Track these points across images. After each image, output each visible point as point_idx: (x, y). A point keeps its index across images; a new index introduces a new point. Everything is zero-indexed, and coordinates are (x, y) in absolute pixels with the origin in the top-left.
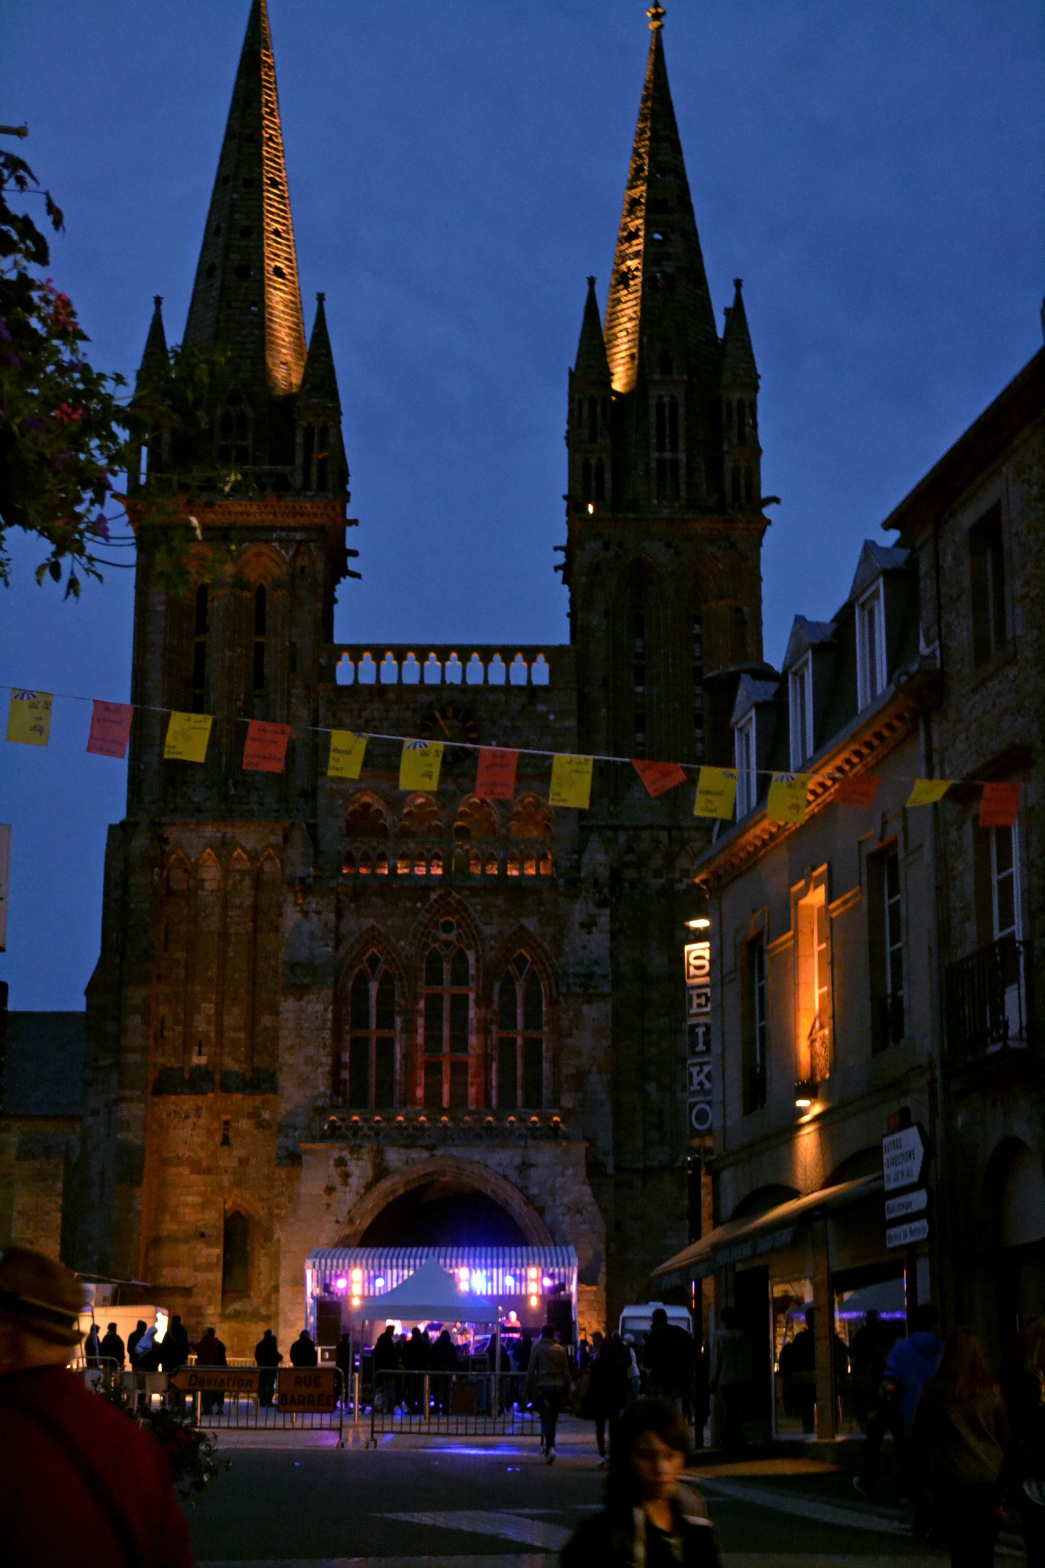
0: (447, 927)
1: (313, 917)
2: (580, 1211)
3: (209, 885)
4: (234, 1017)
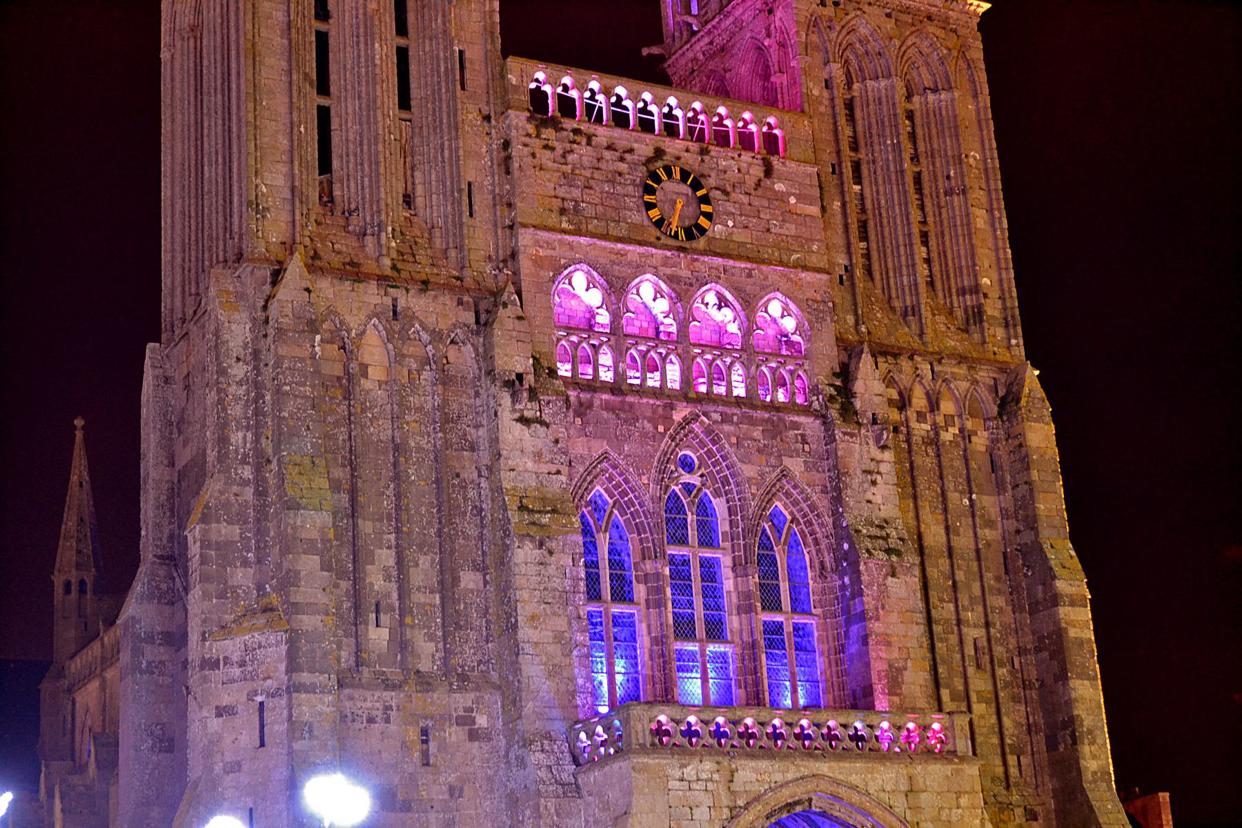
0: (687, 465)
3: (375, 373)
4: (424, 569)
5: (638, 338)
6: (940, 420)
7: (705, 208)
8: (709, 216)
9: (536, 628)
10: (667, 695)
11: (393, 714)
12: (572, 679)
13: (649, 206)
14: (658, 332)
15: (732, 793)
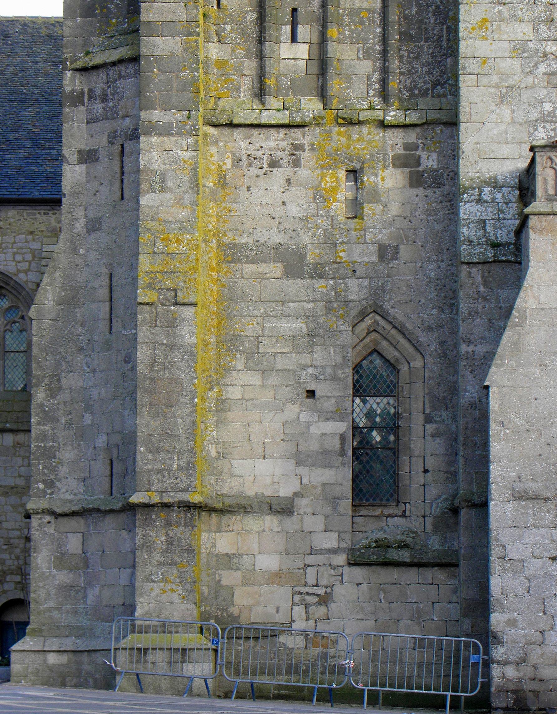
9: (485, 38)
11: (305, 155)
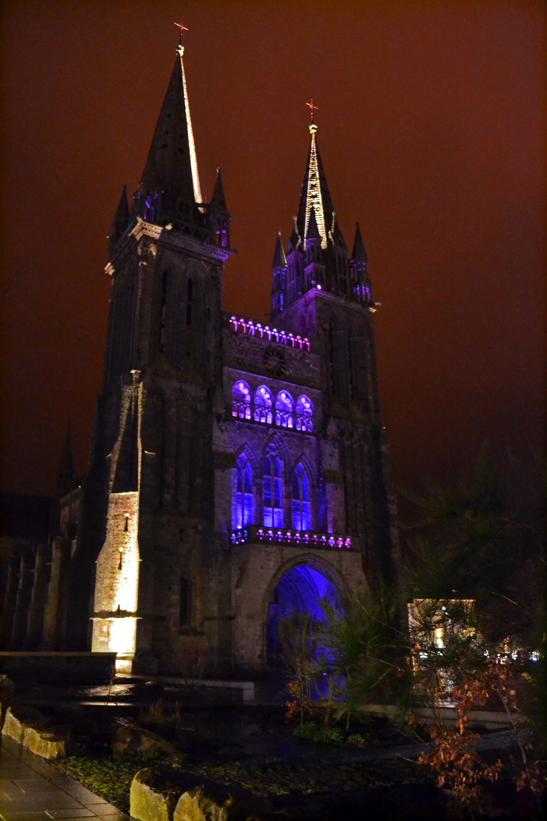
0: (272, 449)
1: (226, 433)
2: (360, 583)
5: (260, 406)
6: (353, 441)
7: (284, 366)
8: (285, 369)
10: (261, 524)
12: (231, 516)
13: (266, 363)
14: (265, 404)
15: (282, 557)
